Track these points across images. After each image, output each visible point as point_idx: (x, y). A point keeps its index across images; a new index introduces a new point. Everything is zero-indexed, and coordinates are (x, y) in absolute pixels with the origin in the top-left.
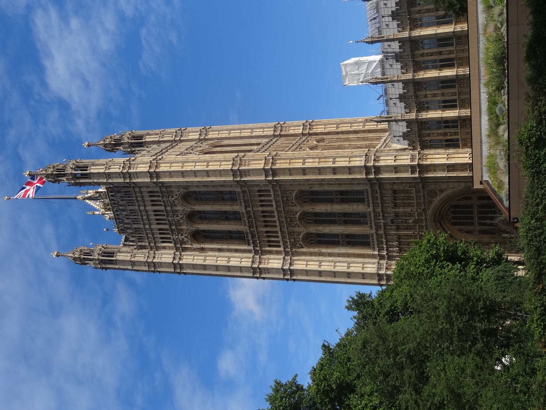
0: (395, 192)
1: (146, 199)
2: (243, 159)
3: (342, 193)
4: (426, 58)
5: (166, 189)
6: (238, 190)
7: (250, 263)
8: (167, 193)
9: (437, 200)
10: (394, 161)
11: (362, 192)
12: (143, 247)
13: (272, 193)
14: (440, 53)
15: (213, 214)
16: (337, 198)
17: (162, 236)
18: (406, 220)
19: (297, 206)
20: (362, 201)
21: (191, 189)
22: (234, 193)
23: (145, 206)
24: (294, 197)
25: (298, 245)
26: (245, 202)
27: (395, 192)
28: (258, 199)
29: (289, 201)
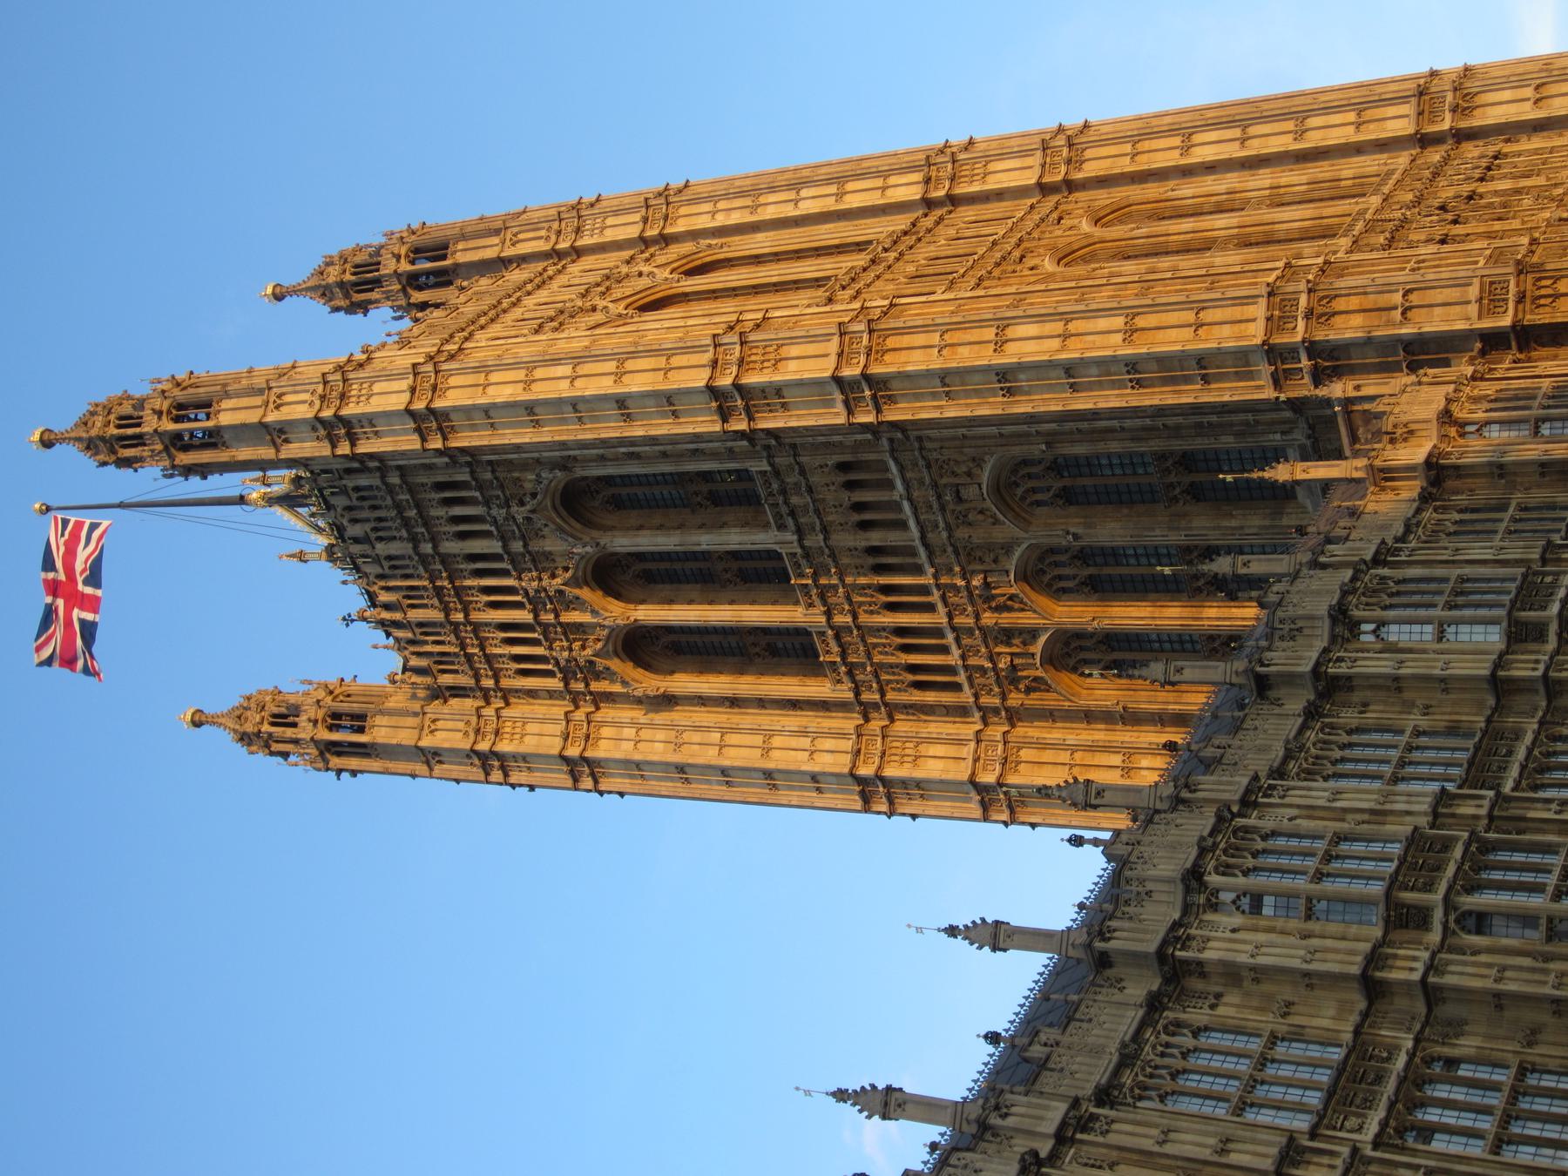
1: (434, 512)
2: (752, 337)
3: (1187, 461)
5: (493, 471)
6: (759, 466)
7: (849, 757)
8: (502, 487)
10: (1403, 313)
15: (679, 560)
16: (1171, 486)
19: (1004, 523)
21: (579, 472)
22: (743, 475)
23: (434, 540)
24: (984, 487)
29: (967, 506)
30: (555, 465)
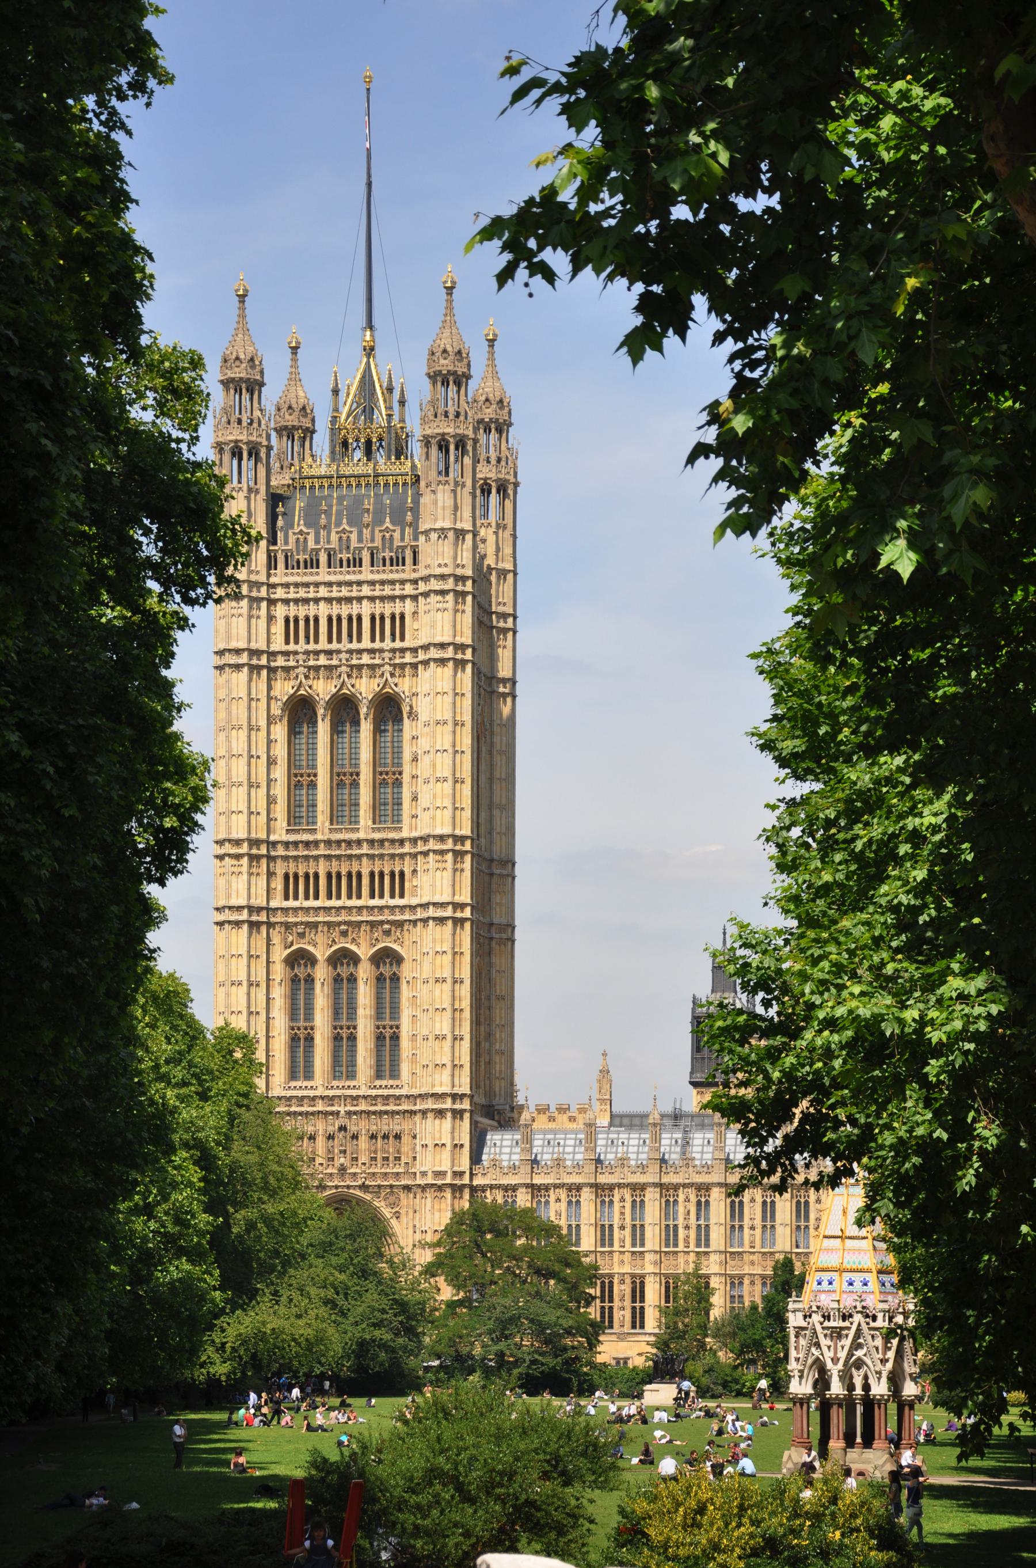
0: (398, 1137)
3: (395, 1038)
4: (617, 1205)
9: (380, 1204)
11: (395, 1074)
12: (271, 563)
13: (397, 901)
14: (622, 1228)
17: (302, 624)
18: (345, 1152)
20: (379, 1075)
21: (406, 721)
25: (290, 938)
26: (382, 842)
27: (398, 1137)
28: (386, 871)
30: (411, 707)
